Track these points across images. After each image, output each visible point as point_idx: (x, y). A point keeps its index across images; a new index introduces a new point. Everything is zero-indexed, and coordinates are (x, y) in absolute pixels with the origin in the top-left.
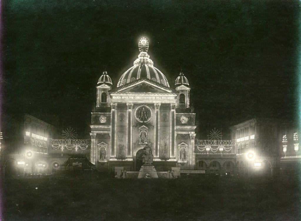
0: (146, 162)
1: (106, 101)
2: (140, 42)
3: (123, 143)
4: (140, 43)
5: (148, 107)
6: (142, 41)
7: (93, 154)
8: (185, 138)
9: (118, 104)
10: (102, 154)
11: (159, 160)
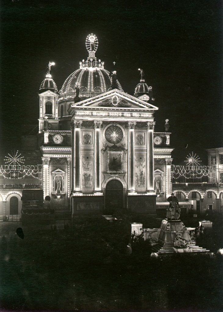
0: (172, 217)
1: (51, 113)
2: (88, 38)
3: (88, 172)
4: (87, 40)
5: (118, 125)
6: (89, 38)
7: (46, 184)
8: (160, 163)
9: (83, 121)
10: (58, 185)
11: (136, 194)
